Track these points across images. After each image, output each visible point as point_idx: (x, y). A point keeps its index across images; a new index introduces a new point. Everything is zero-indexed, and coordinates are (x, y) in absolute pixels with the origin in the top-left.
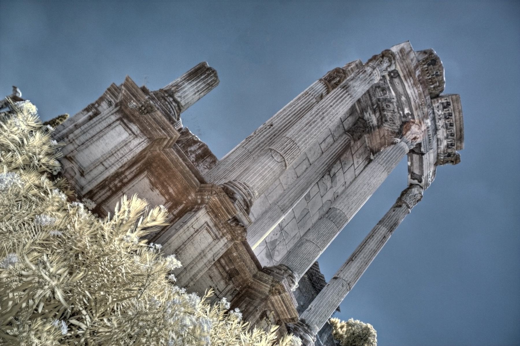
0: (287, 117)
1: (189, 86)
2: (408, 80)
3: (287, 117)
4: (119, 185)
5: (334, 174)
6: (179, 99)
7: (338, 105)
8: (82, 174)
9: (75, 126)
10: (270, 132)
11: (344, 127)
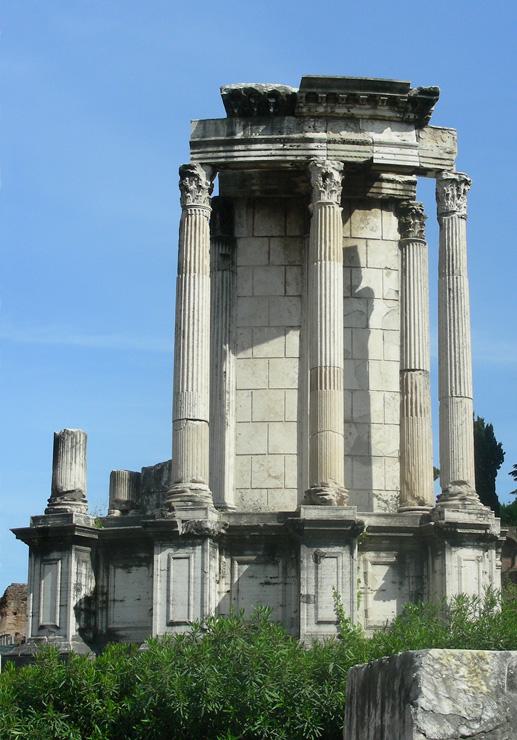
4: (104, 597)
11: (292, 237)
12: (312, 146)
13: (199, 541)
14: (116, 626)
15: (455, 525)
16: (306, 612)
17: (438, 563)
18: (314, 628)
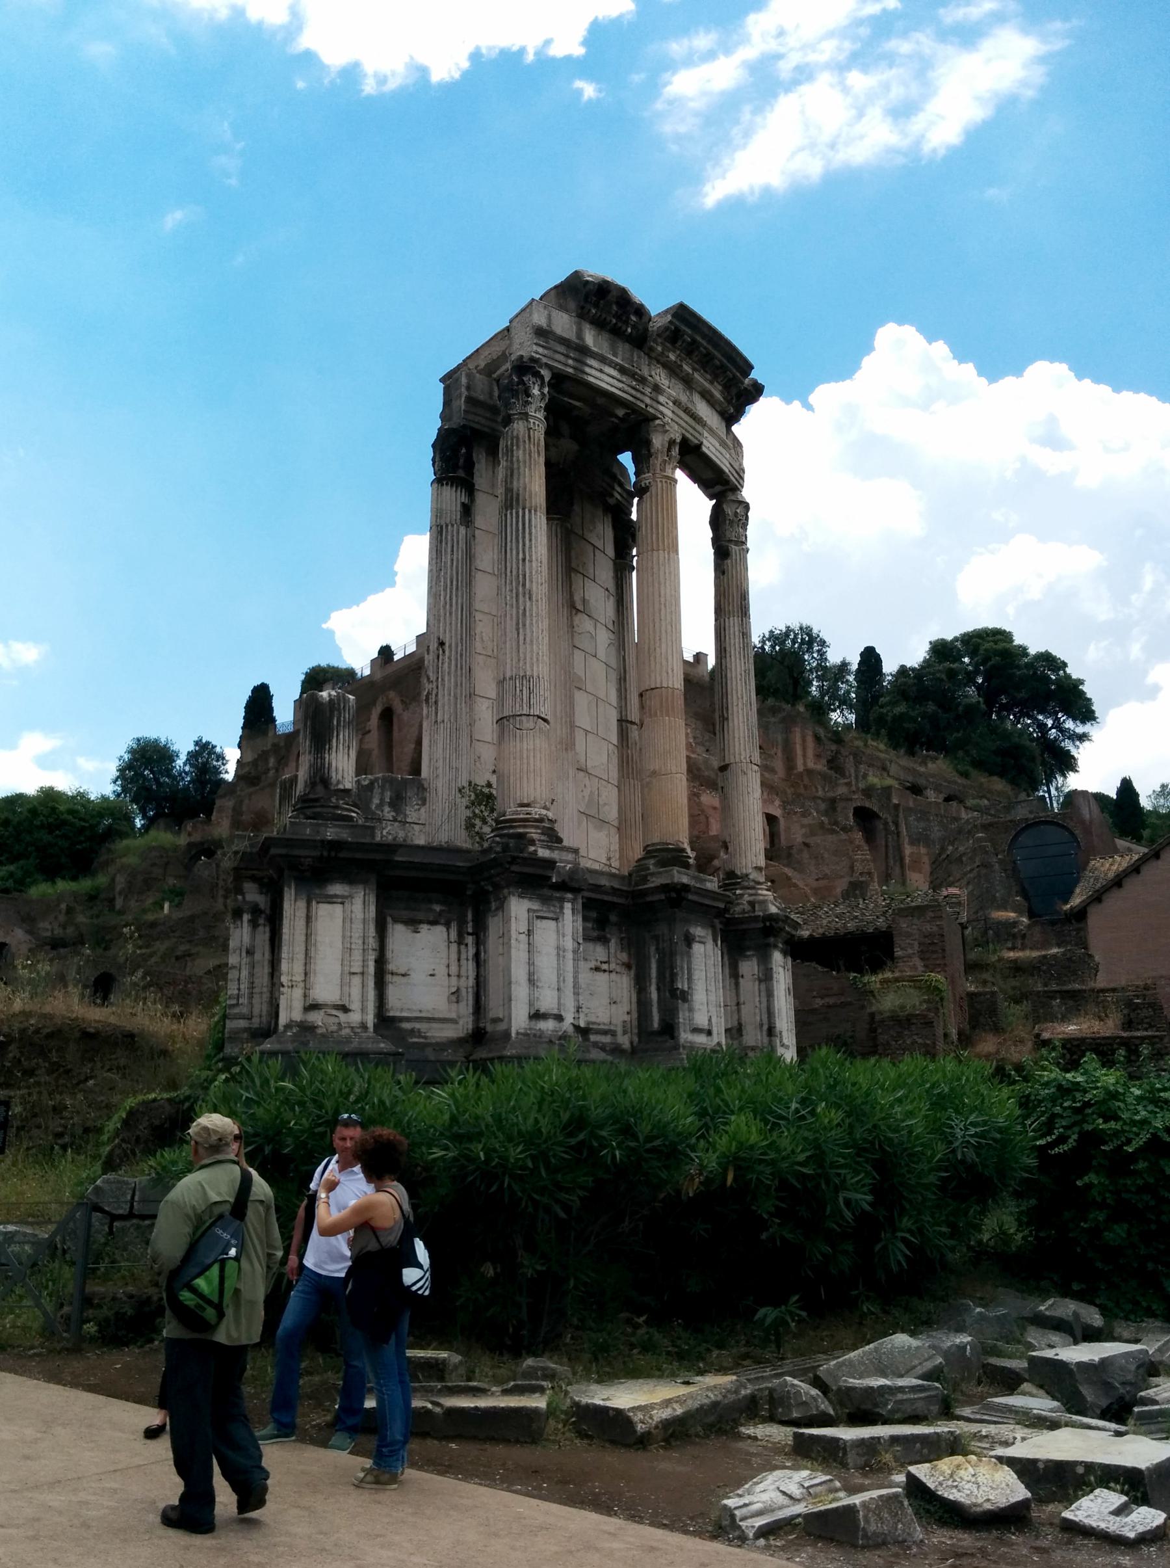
0: (451, 605)
1: (334, 754)
2: (587, 370)
3: (451, 605)
5: (584, 600)
6: (341, 787)
7: (530, 547)
8: (345, 1009)
9: (248, 952)
10: (449, 658)
13: (569, 896)
14: (398, 1014)
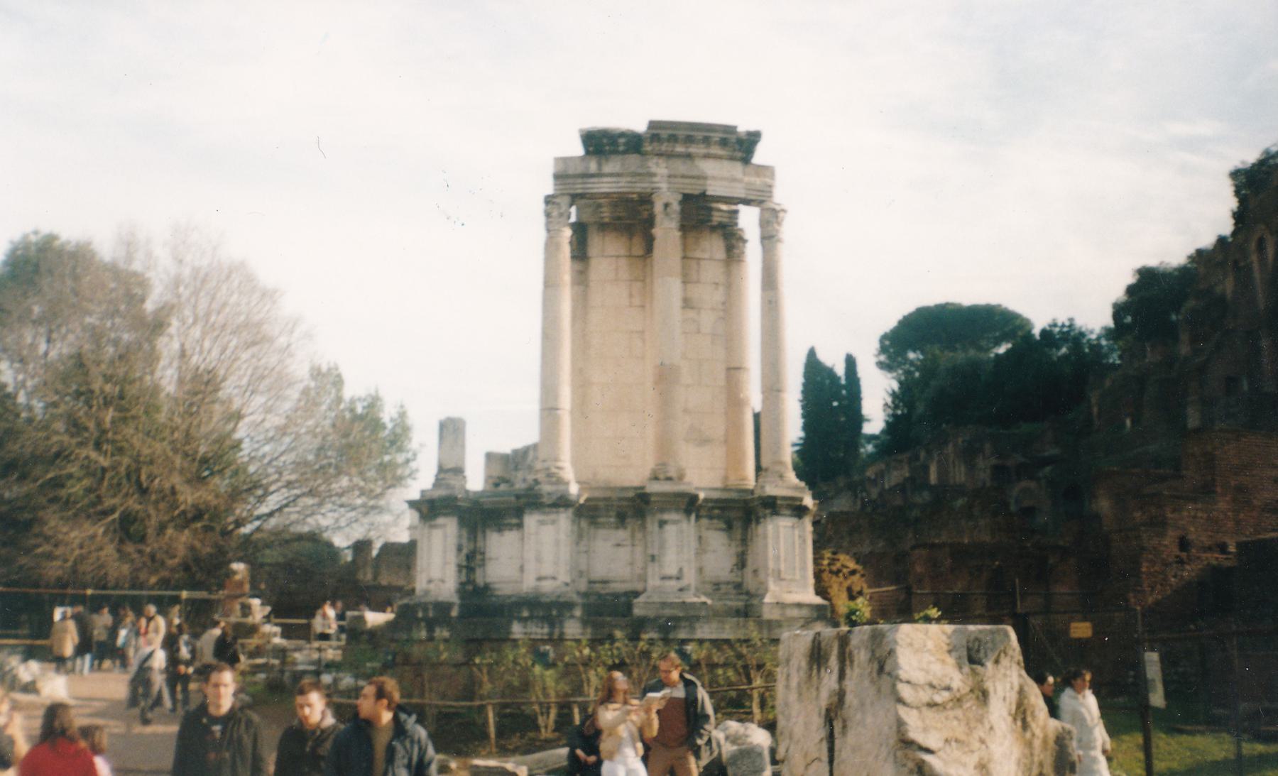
12: (656, 179)
15: (774, 498)
16: (653, 570)
17: (760, 529)
18: (658, 582)
